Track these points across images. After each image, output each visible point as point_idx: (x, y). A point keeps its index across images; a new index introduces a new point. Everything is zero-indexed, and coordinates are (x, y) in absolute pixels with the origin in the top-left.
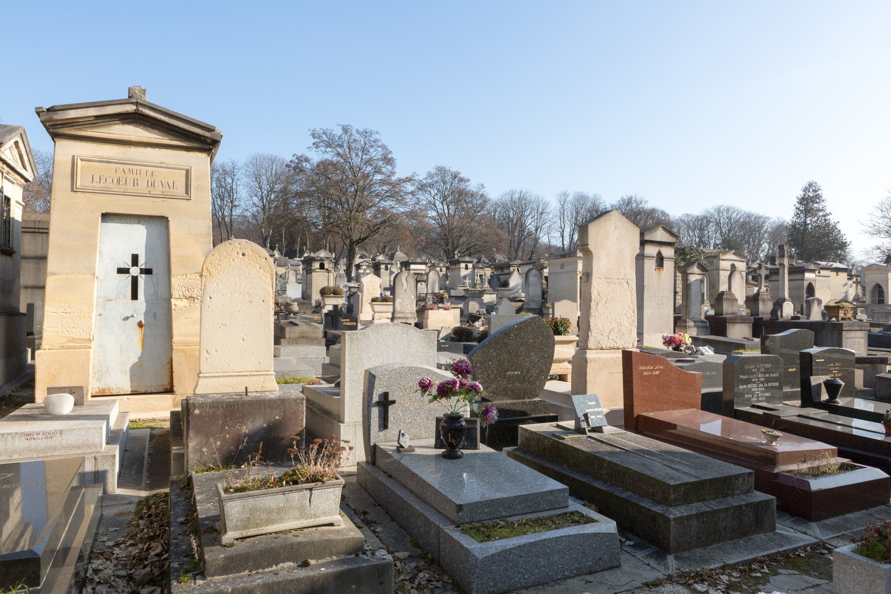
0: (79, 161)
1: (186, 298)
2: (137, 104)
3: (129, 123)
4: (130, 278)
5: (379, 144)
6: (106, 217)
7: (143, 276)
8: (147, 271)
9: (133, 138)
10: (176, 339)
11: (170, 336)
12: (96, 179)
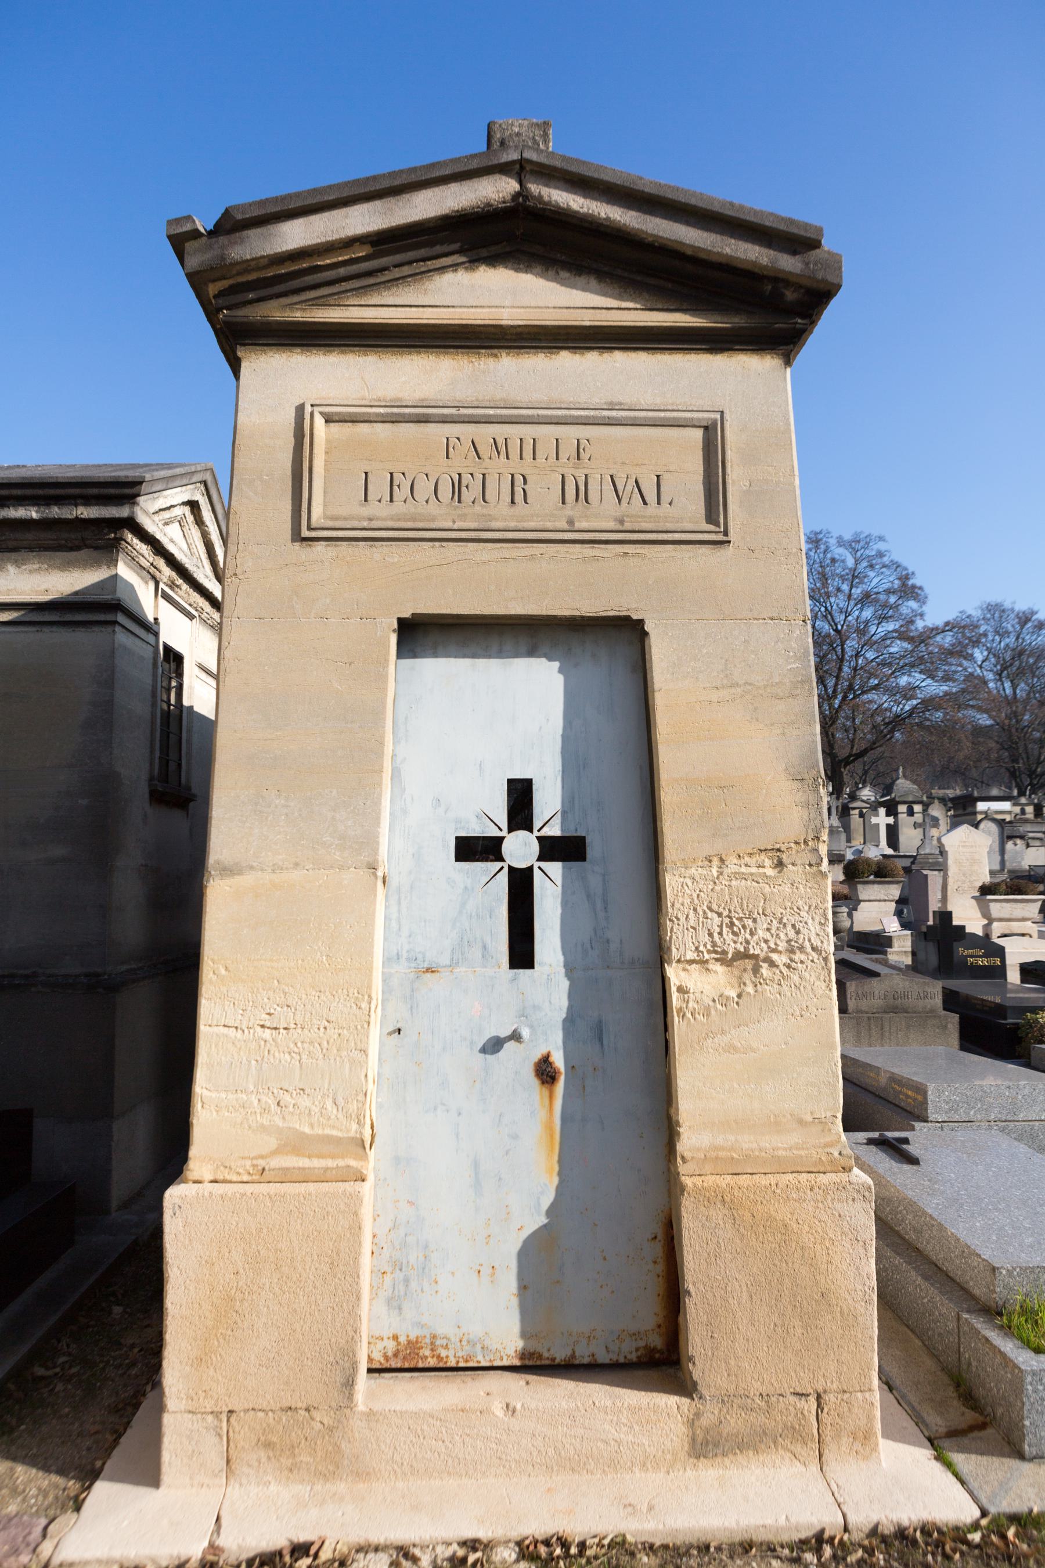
0: (319, 421)
1: (723, 959)
2: (520, 169)
3: (493, 260)
4: (504, 878)
5: (886, 560)
6: (418, 634)
7: (555, 868)
8: (561, 849)
9: (509, 316)
10: (688, 1142)
11: (668, 1131)
12: (379, 487)
